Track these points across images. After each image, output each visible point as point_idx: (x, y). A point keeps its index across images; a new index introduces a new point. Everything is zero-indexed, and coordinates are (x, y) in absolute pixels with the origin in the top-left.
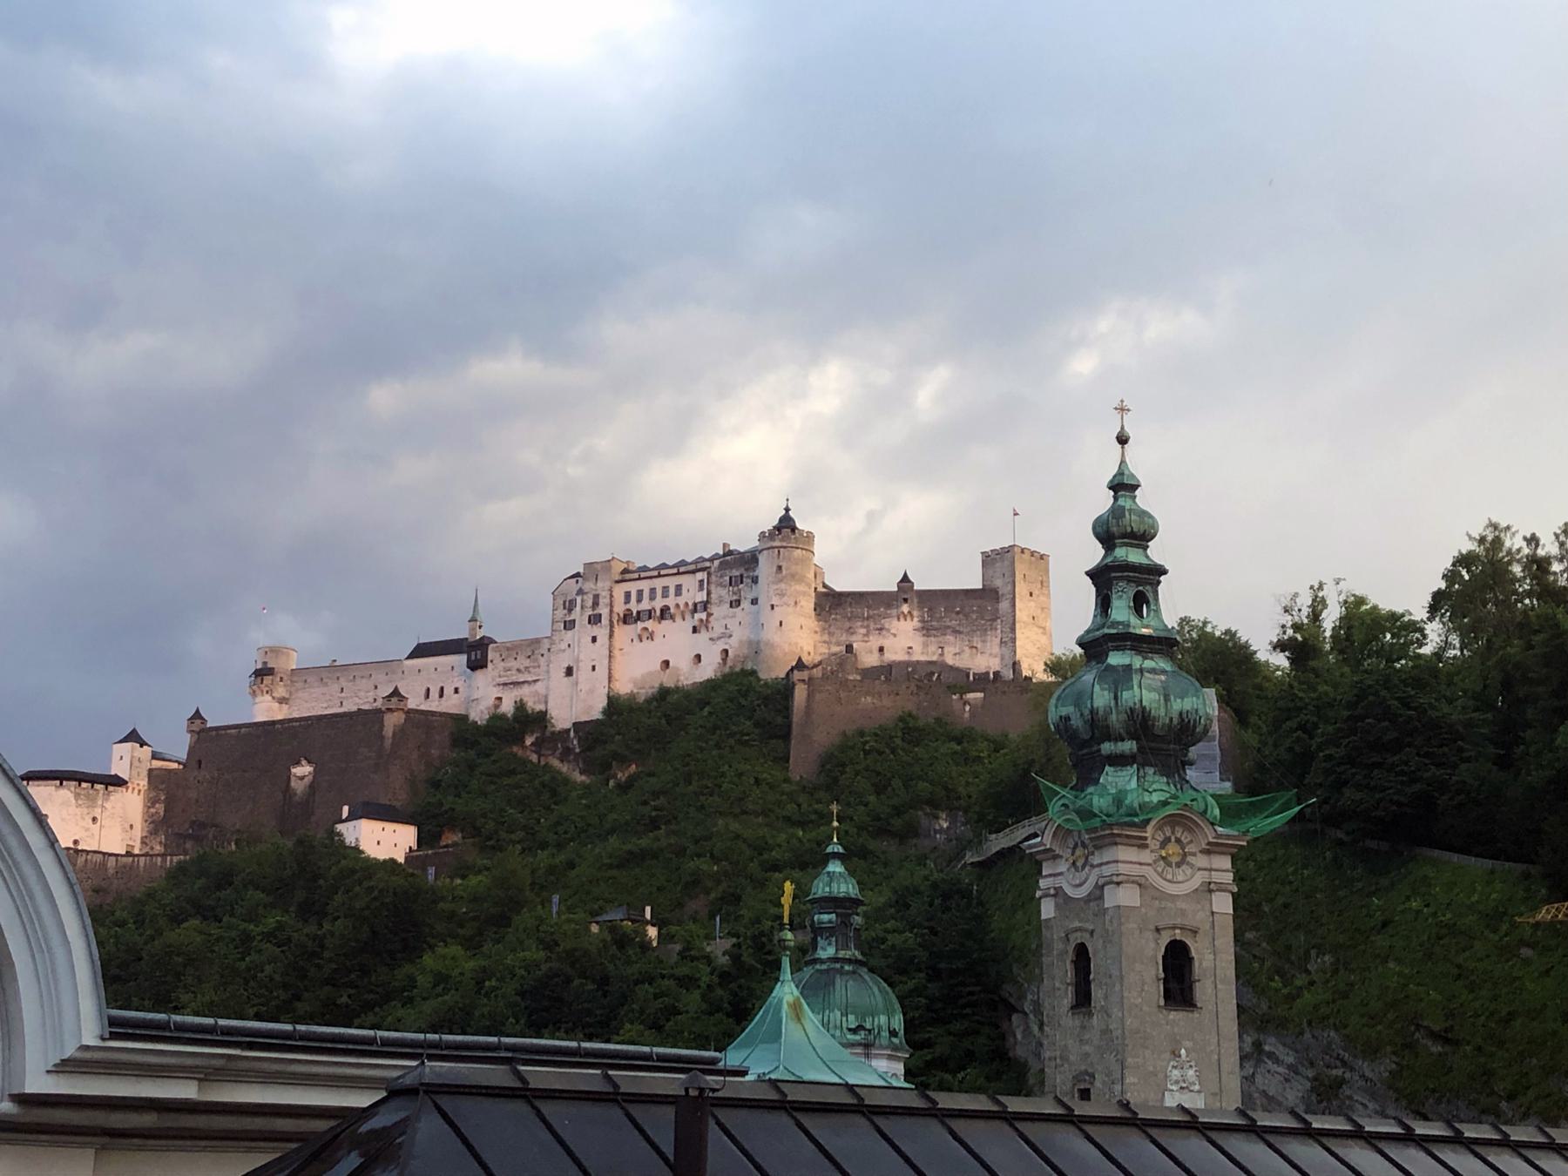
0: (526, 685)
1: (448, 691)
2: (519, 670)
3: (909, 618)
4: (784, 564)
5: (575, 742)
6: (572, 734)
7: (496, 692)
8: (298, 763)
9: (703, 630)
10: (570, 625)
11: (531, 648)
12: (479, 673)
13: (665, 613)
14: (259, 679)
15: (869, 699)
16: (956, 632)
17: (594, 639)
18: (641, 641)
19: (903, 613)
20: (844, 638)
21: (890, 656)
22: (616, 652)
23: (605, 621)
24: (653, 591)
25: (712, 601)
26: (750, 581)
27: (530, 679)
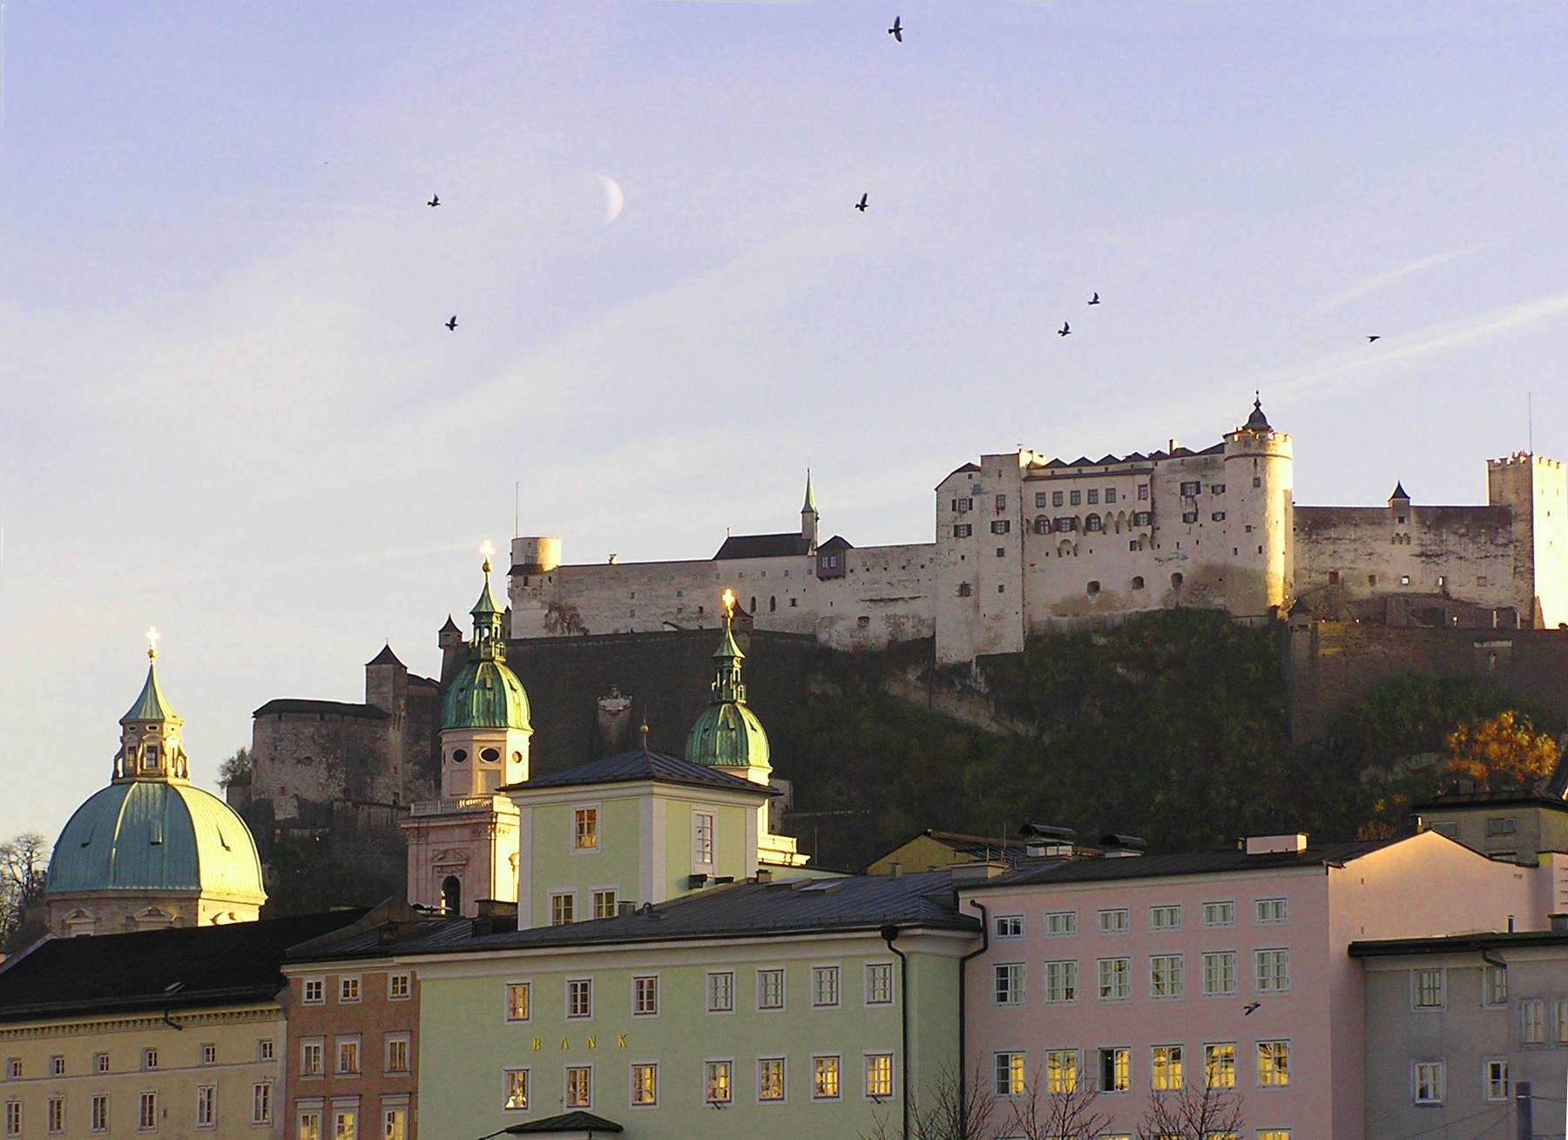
0: (901, 603)
1: (783, 603)
3: (1404, 542)
5: (981, 679)
6: (974, 666)
8: (607, 694)
9: (1147, 549)
11: (905, 555)
12: (833, 584)
13: (1092, 523)
14: (521, 579)
15: (1379, 647)
16: (1461, 558)
17: (1001, 552)
18: (1060, 556)
19: (1398, 534)
20: (1327, 563)
22: (1028, 569)
23: (1015, 527)
24: (1075, 496)
25: (1157, 512)
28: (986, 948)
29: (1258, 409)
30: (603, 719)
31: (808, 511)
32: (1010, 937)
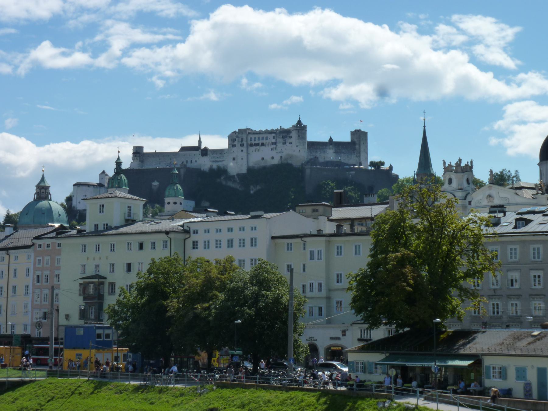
1: (194, 161)
2: (217, 157)
4: (300, 135)
5: (237, 179)
6: (236, 176)
7: (211, 163)
8: (154, 181)
9: (274, 150)
10: (234, 146)
13: (263, 144)
14: (135, 155)
16: (344, 153)
17: (242, 151)
21: (327, 159)
24: (259, 138)
26: (288, 137)
27: (221, 160)
28: (190, 237)
29: (299, 119)
30: (153, 187)
31: (200, 142)
32: (195, 234)
